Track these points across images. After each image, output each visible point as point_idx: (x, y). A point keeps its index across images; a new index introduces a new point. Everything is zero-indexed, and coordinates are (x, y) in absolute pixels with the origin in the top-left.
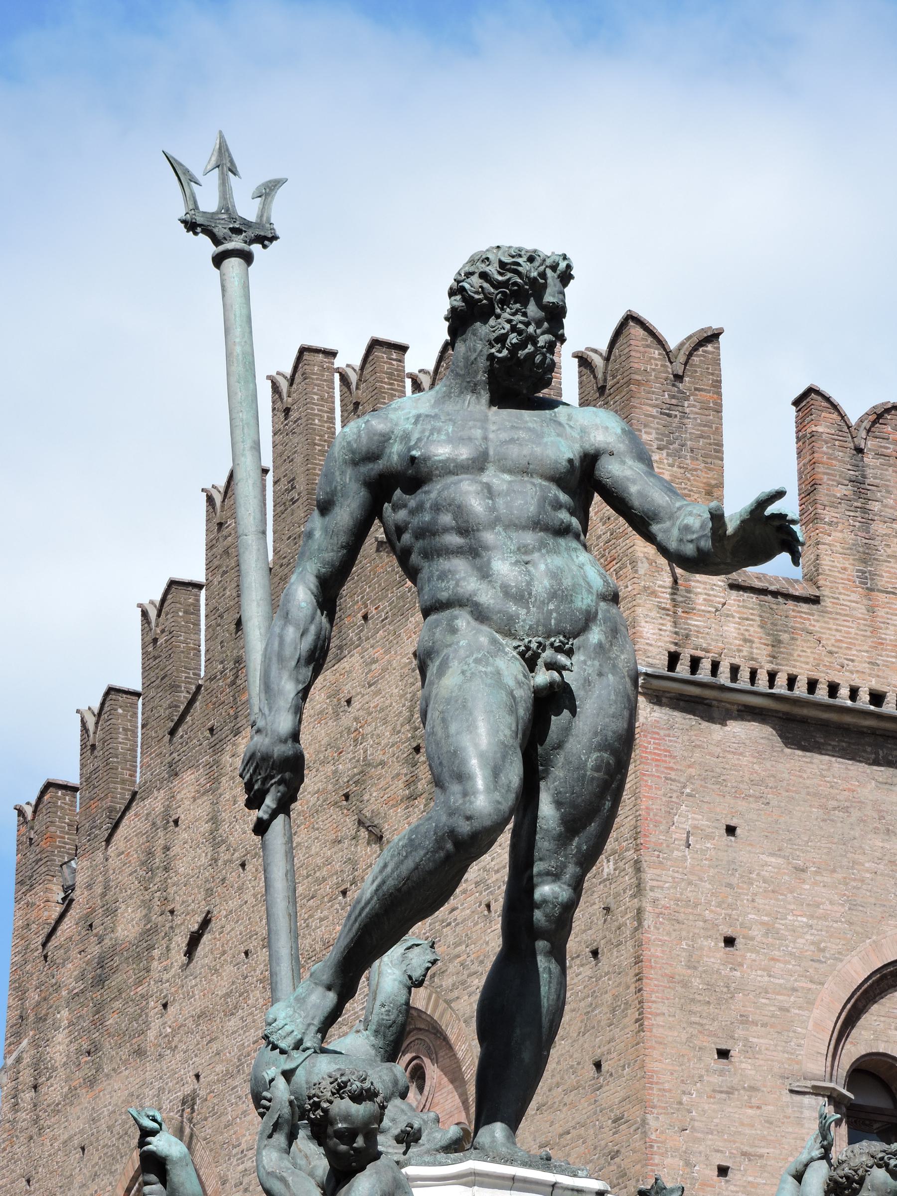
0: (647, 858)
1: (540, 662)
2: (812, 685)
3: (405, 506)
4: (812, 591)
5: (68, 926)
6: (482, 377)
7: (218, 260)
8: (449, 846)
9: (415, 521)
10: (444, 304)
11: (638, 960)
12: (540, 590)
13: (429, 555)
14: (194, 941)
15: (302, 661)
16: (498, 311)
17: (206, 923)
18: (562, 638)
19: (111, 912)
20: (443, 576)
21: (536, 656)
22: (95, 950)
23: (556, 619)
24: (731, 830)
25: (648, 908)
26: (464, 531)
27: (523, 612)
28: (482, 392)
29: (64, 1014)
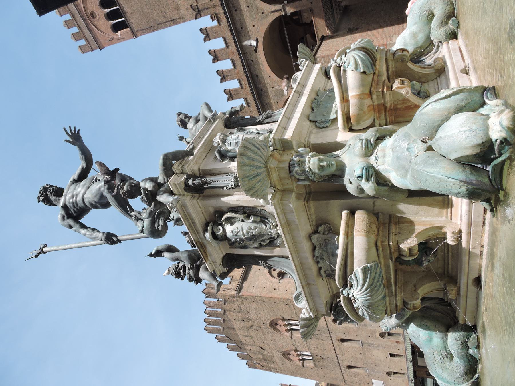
0: (255, 295)
2: (241, 277)
3: (71, 210)
4: (232, 277)
5: (261, 364)
6: (57, 198)
8: (110, 190)
9: (72, 207)
10: (48, 206)
11: (265, 297)
13: (77, 205)
14: (262, 349)
17: (260, 347)
19: (259, 358)
22: (263, 360)
24: (253, 286)
25: (259, 295)
26: (73, 196)
29: (269, 365)
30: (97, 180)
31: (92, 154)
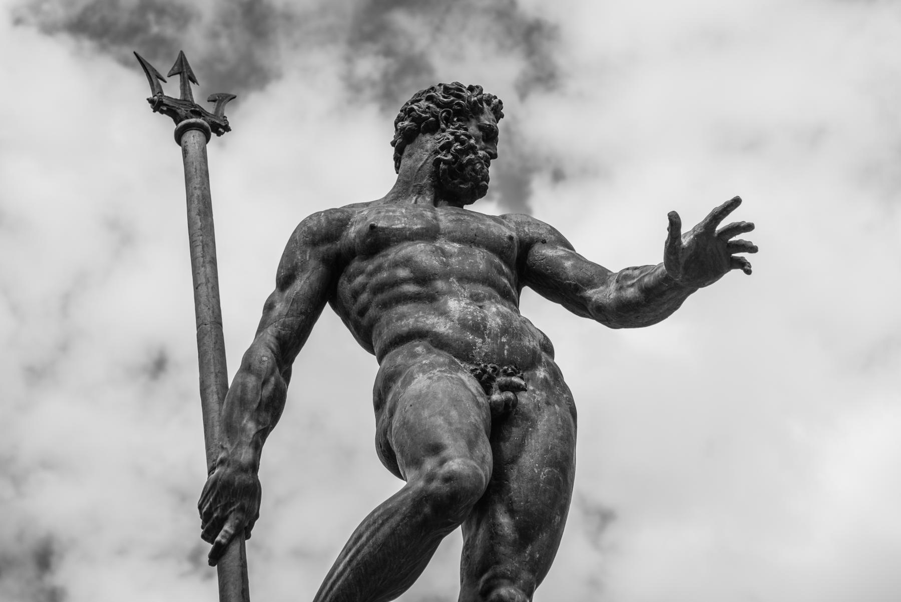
1: (495, 385)
3: (361, 272)
6: (426, 181)
7: (179, 136)
9: (374, 280)
12: (494, 325)
13: (386, 305)
15: (263, 406)
16: (443, 126)
18: (513, 367)
20: (402, 317)
21: (491, 379)
23: (508, 350)
26: (423, 278)
27: (480, 340)
28: (428, 192)
30: (510, 395)
31: (666, 319)
